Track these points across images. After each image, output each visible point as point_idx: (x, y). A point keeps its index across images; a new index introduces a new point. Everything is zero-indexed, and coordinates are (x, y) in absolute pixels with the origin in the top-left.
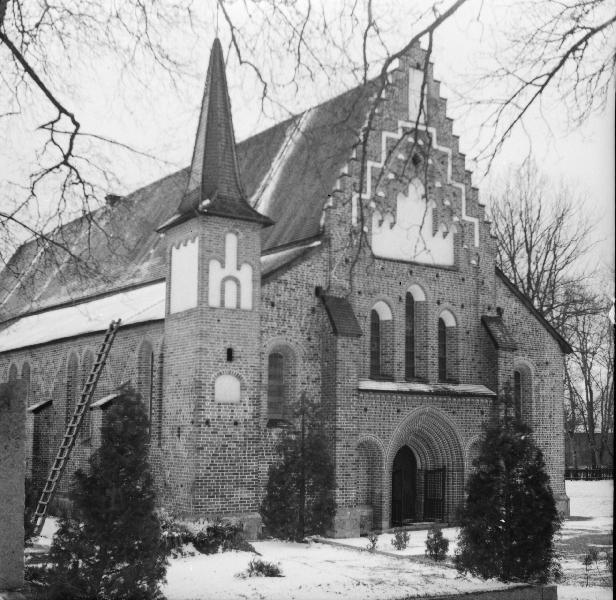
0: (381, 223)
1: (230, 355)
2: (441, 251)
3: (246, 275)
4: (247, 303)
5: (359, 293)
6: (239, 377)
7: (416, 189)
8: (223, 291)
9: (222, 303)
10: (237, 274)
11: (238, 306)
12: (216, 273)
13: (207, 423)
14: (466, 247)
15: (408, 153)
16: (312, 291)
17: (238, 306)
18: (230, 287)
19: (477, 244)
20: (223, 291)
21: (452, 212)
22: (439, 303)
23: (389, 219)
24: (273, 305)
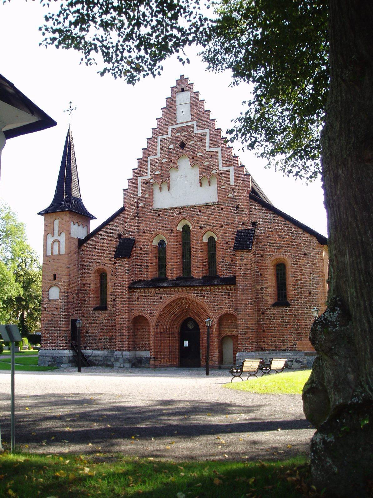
0: (161, 189)
1: (55, 275)
2: (208, 195)
3: (62, 239)
4: (63, 251)
5: (144, 232)
6: (59, 287)
7: (184, 163)
8: (52, 248)
9: (52, 252)
10: (58, 238)
11: (59, 254)
12: (50, 240)
13: (45, 309)
14: (223, 187)
15: (175, 144)
16: (116, 237)
17: (59, 254)
18: (56, 246)
19: (232, 183)
20: (52, 248)
21: (210, 168)
22: (201, 228)
23: (165, 187)
24: (95, 248)
